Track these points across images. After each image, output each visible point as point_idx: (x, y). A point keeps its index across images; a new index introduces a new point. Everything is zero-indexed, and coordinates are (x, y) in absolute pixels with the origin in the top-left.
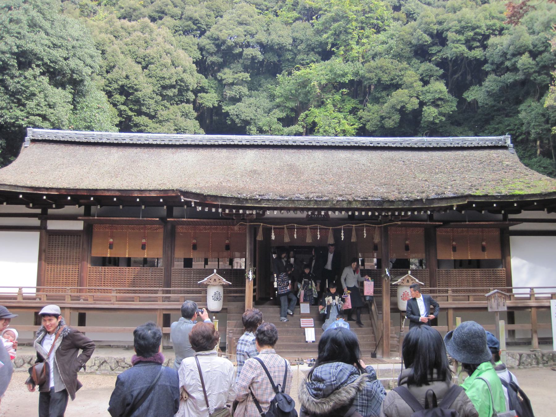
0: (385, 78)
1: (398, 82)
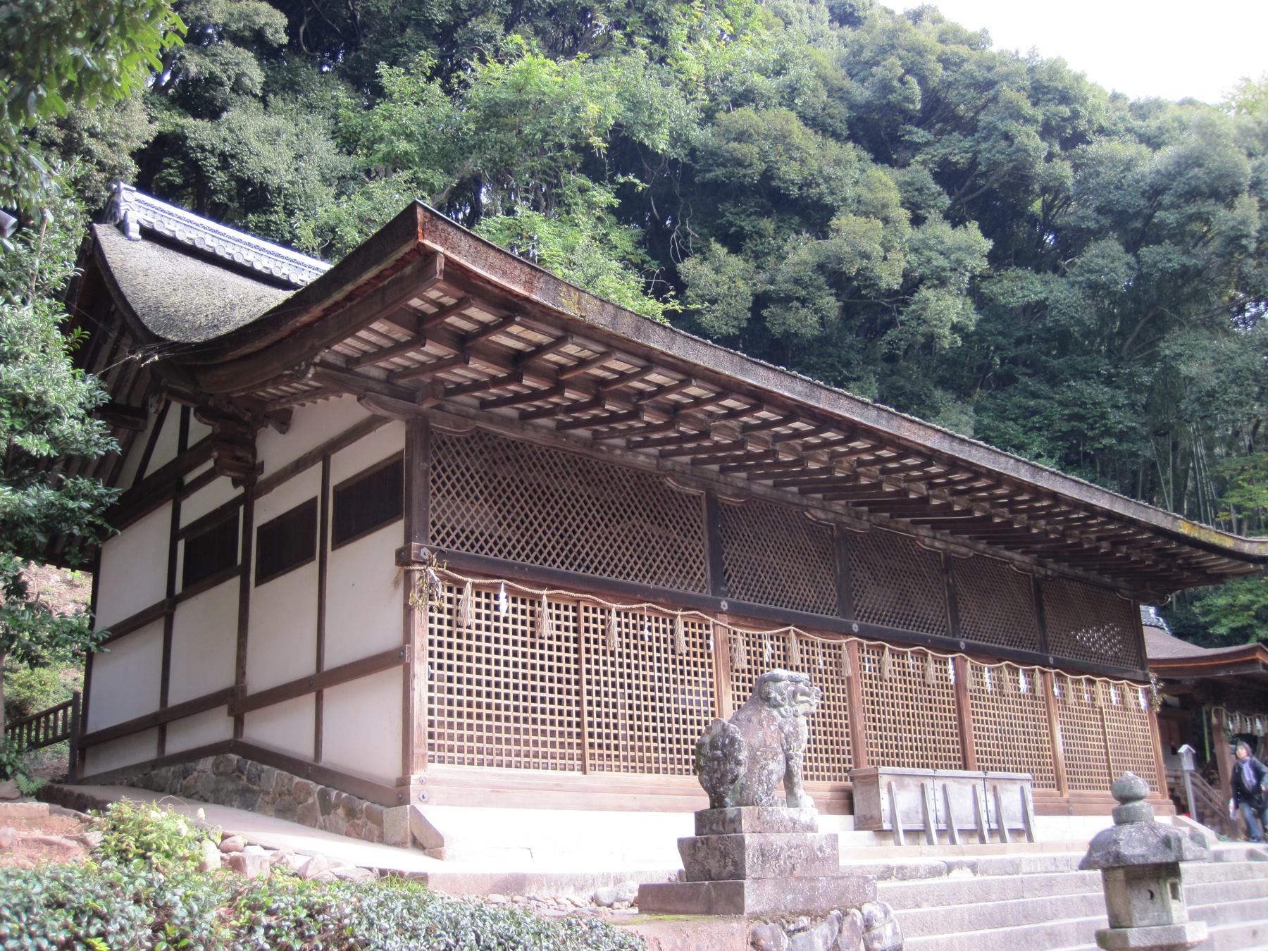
0: (790, 172)
1: (821, 195)
